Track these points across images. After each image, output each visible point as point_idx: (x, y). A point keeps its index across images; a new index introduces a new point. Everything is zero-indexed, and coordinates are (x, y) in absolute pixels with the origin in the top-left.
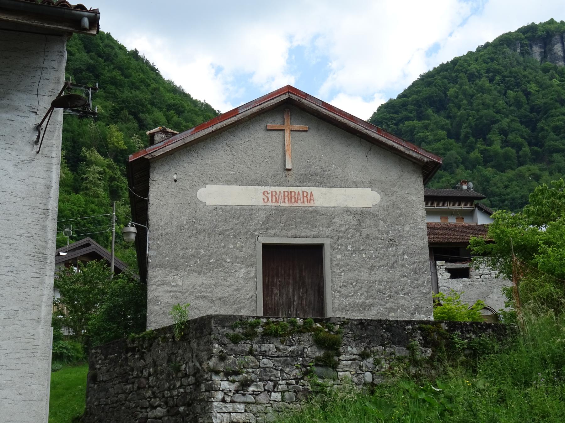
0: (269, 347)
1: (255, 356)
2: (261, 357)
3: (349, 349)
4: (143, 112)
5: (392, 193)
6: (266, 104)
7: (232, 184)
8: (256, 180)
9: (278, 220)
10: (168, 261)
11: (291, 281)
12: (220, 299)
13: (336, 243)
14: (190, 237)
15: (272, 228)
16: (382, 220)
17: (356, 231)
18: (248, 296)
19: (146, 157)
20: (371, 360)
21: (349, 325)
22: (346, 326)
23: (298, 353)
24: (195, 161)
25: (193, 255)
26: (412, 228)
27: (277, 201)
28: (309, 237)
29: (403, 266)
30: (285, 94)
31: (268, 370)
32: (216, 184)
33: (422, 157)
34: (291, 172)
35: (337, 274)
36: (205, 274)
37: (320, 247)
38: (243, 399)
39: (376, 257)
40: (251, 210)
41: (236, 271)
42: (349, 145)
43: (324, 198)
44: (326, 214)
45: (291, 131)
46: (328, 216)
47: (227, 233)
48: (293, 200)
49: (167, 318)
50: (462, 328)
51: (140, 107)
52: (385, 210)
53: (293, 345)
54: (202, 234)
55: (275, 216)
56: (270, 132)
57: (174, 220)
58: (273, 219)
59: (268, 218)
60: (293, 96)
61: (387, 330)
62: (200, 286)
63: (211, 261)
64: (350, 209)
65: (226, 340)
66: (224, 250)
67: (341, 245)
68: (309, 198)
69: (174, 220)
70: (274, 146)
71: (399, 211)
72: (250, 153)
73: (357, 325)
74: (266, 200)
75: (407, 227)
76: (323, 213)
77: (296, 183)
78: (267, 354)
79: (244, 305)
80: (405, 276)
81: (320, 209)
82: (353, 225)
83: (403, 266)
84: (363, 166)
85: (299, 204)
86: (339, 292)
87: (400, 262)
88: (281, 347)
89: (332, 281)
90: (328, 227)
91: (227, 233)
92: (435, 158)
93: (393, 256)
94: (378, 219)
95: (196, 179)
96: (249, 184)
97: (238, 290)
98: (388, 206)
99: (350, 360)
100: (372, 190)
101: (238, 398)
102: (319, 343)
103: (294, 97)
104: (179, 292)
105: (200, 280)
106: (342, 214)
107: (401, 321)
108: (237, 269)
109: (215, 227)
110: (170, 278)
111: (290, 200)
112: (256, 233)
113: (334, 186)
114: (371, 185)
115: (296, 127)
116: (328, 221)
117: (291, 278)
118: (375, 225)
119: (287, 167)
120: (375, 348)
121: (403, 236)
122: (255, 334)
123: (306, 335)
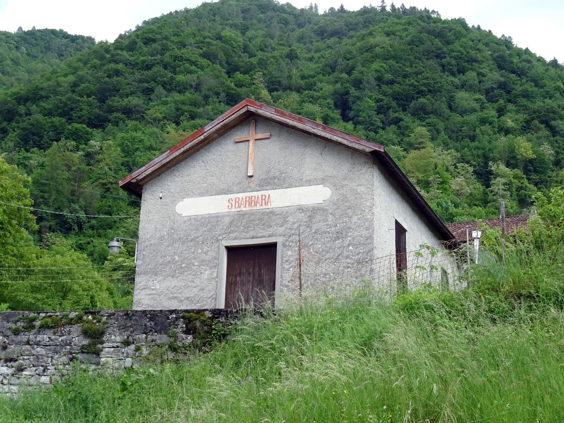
0: (44, 337)
1: (31, 345)
2: (36, 346)
3: (113, 337)
4: (554, 119)
5: (342, 187)
6: (230, 118)
7: (204, 196)
8: (224, 189)
9: (239, 224)
10: (150, 268)
11: (251, 279)
12: (188, 298)
13: (287, 240)
14: (168, 246)
15: (233, 232)
16: (331, 214)
17: (307, 227)
18: (210, 295)
19: (132, 181)
20: (133, 347)
21: (115, 316)
22: (112, 317)
23: (66, 342)
24: (176, 179)
25: (169, 262)
26: (359, 219)
27: (239, 207)
28: (264, 237)
29: (347, 257)
30: (244, 107)
31: (40, 357)
32: (192, 197)
33: (365, 148)
34: (253, 179)
35: (286, 270)
36: (177, 277)
37: (273, 246)
38: (17, 382)
39: (323, 251)
40: (218, 217)
41: (201, 273)
42: (306, 146)
43: (281, 199)
44: (281, 214)
45: (256, 140)
46: (282, 215)
47: (197, 240)
48: (253, 204)
50: (227, 315)
51: (551, 115)
52: (334, 204)
53: (63, 335)
54: (177, 243)
55: (240, 219)
56: (238, 144)
57: (158, 232)
58: (235, 223)
59: (231, 223)
60: (251, 108)
61: (151, 319)
63: (183, 265)
64: (302, 206)
65: (9, 333)
66: (193, 255)
67: (292, 242)
68: (266, 200)
69: (158, 232)
70: (241, 156)
71: (348, 204)
72: (220, 165)
73: (123, 316)
74: (230, 207)
75: (355, 219)
76: (279, 213)
77: (257, 188)
78: (41, 343)
79: (206, 303)
80: (349, 267)
81: (275, 210)
82: (304, 222)
83: (347, 257)
84: (318, 164)
85: (258, 207)
86: (287, 286)
87: (345, 254)
88: (53, 337)
89: (282, 277)
90: (282, 226)
91: (197, 240)
92: (376, 147)
93: (339, 248)
94: (327, 214)
95: (176, 195)
96: (218, 194)
97: (202, 290)
98: (338, 200)
99: (113, 347)
100: (324, 186)
101: (14, 380)
102: (86, 333)
104: (156, 294)
105: (173, 283)
106: (295, 212)
107: (165, 311)
108: (203, 271)
109: (188, 236)
110: (150, 283)
111: (250, 204)
112: (221, 238)
113: (290, 186)
114: (323, 181)
115: (260, 136)
116: (282, 220)
117: (252, 276)
118: (324, 219)
119: (249, 175)
120: (137, 336)
121: (350, 228)
122: (33, 327)
123: (76, 326)
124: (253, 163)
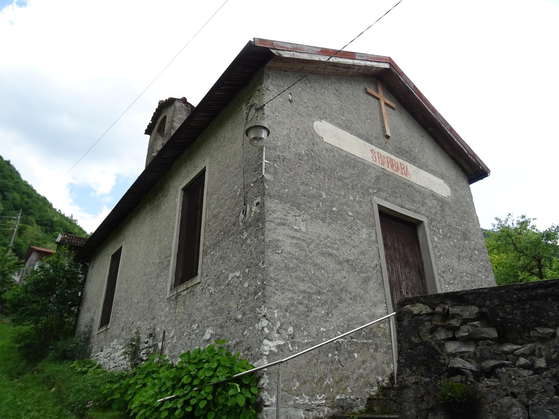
4: (7, 191)
36: (329, 224)
49: (291, 276)
51: (6, 189)
62: (325, 239)
63: (334, 209)
103: (393, 69)
104: (303, 240)
124: (389, 123)
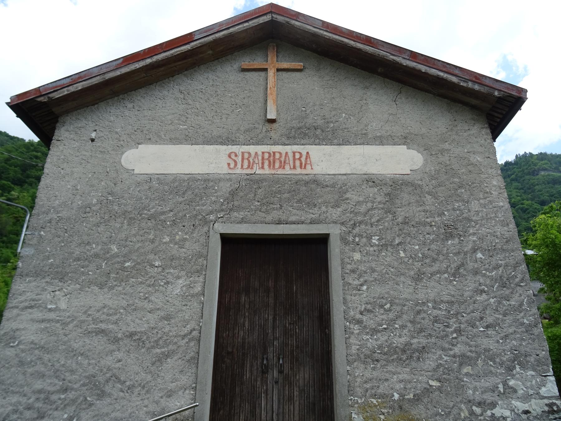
5: (442, 151)
8: (220, 137)
10: (52, 264)
11: (271, 301)
12: (132, 335)
13: (350, 232)
15: (239, 209)
16: (429, 193)
18: (186, 331)
24: (127, 113)
25: (96, 255)
28: (303, 223)
29: (476, 272)
32: (156, 143)
34: (275, 125)
36: (111, 288)
37: (322, 240)
39: (425, 256)
40: (207, 180)
41: (168, 283)
43: (327, 160)
44: (333, 186)
45: (278, 70)
46: (337, 189)
47: (162, 217)
48: (277, 165)
49: (24, 374)
52: (432, 178)
54: (119, 220)
55: (246, 190)
57: (78, 197)
58: (241, 194)
59: (233, 194)
62: (98, 311)
63: (127, 264)
64: (373, 177)
66: (152, 246)
67: (360, 236)
69: (78, 197)
70: (250, 91)
71: (456, 180)
74: (232, 166)
75: (475, 206)
76: (328, 183)
77: (284, 140)
79: (174, 347)
80: (483, 291)
82: (380, 203)
85: (287, 170)
86: (359, 322)
87: (471, 265)
89: (345, 302)
91: (162, 217)
93: (456, 254)
94: (422, 192)
97: (168, 318)
98: (438, 172)
100: (408, 148)
103: (280, 18)
104: (58, 321)
105: (99, 299)
108: (170, 278)
109: (144, 209)
111: (272, 165)
112: (212, 217)
113: (345, 142)
114: (406, 140)
115: (285, 65)
116: (336, 197)
117: (272, 294)
118: (417, 201)
119: (269, 117)
121: (469, 220)
124: (276, 102)
